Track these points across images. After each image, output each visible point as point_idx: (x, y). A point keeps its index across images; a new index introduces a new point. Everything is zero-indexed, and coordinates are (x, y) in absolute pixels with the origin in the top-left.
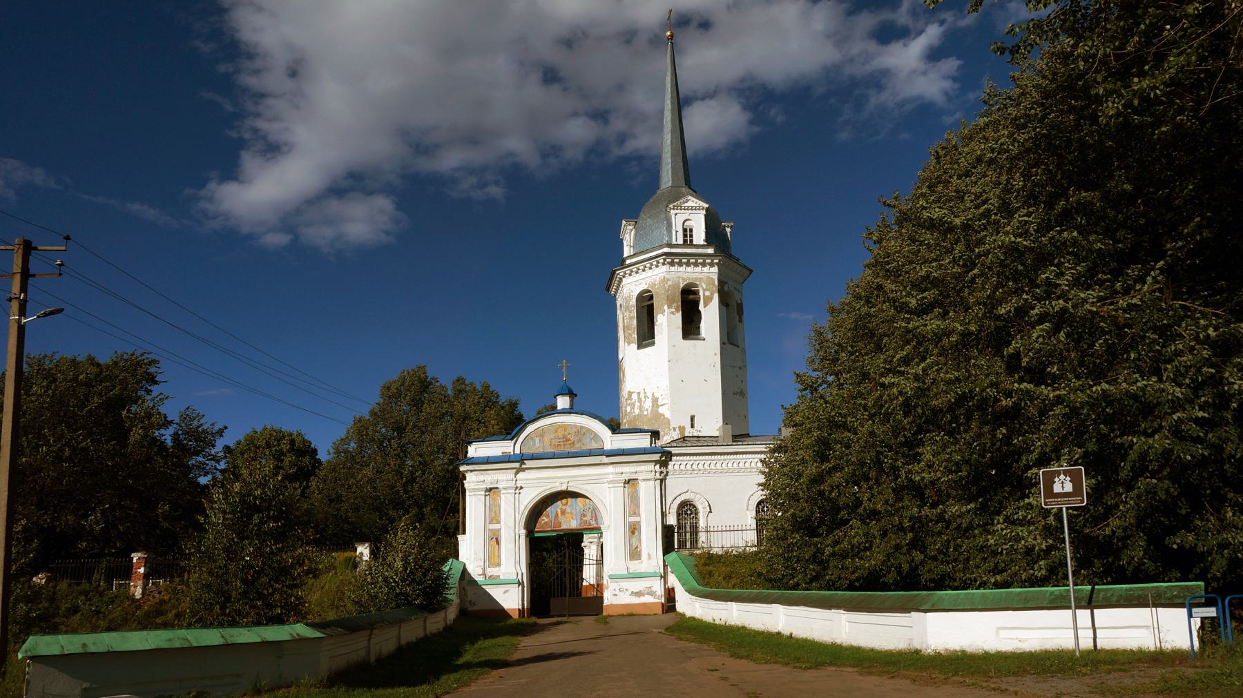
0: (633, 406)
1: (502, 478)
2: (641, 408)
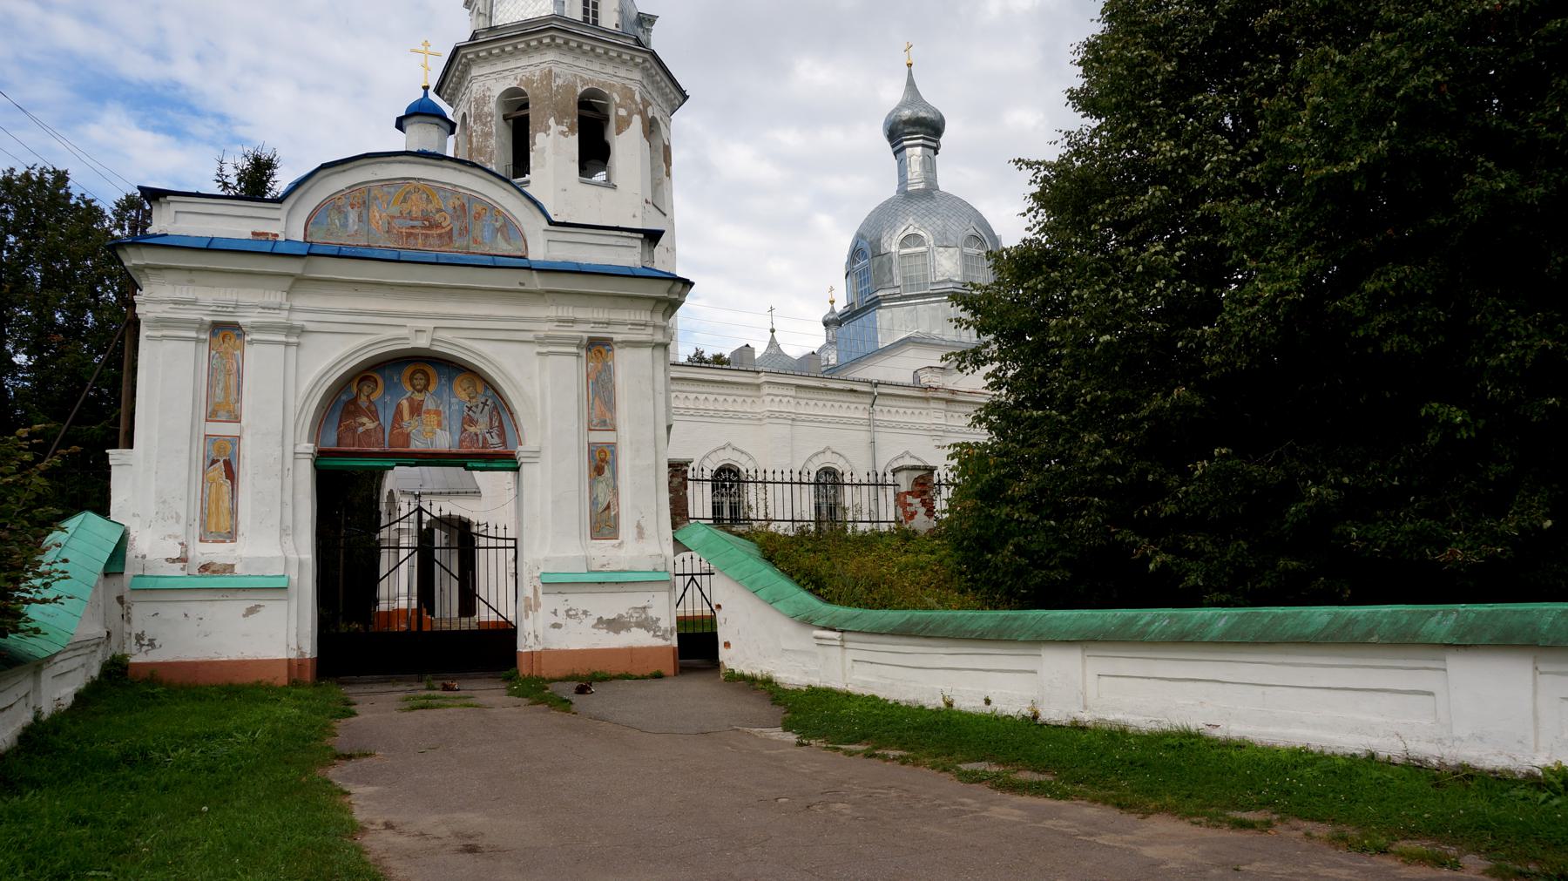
1: (251, 302)
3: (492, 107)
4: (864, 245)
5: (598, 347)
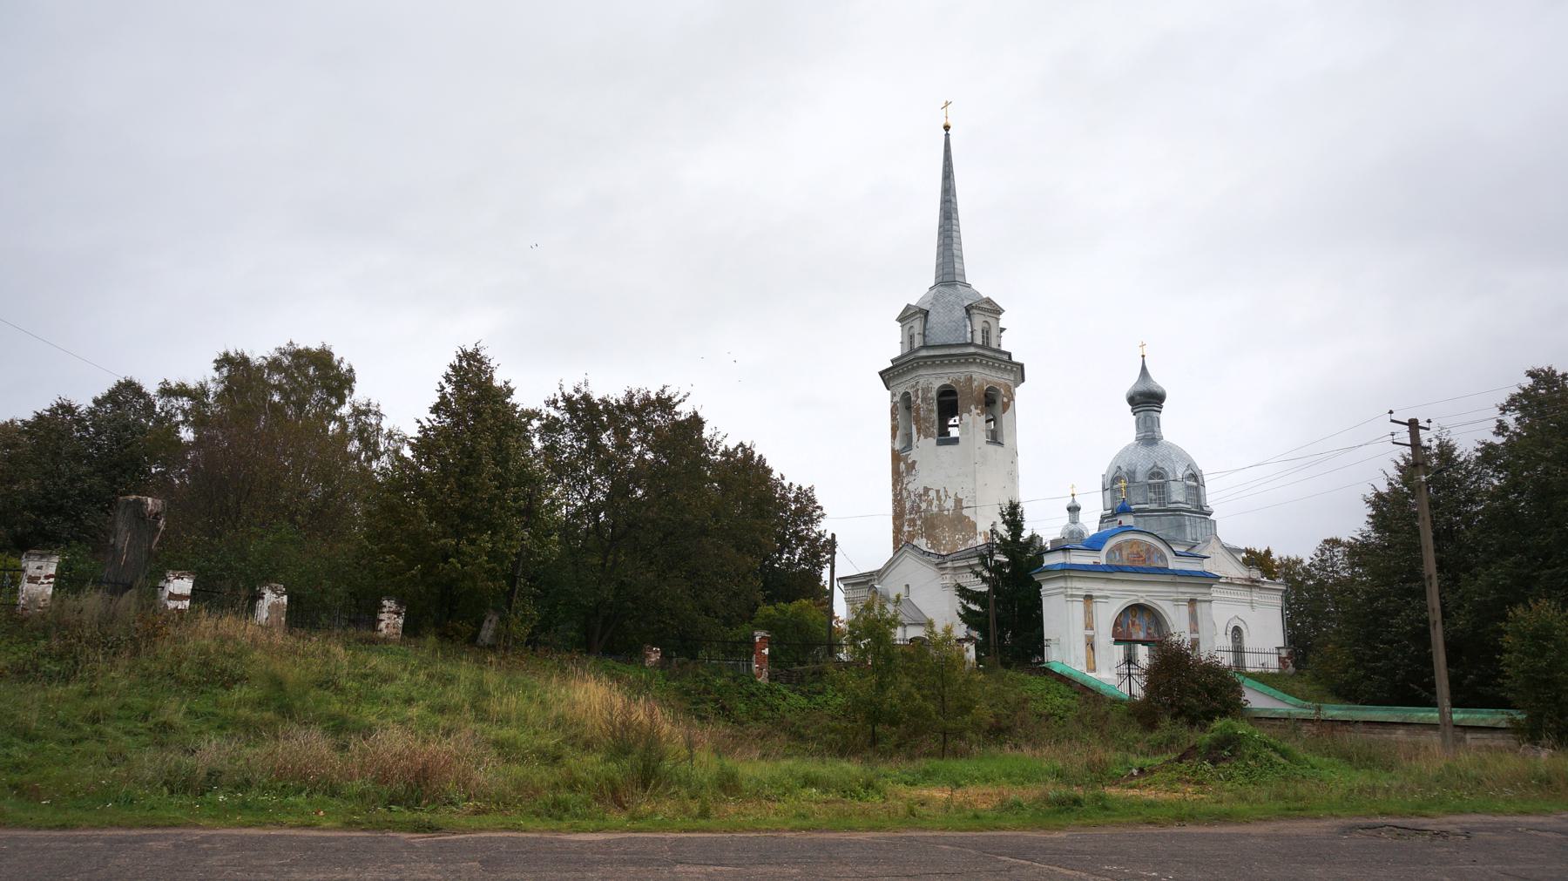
0: (930, 503)
1: (1095, 587)
2: (940, 506)
3: (934, 394)
5: (1192, 602)
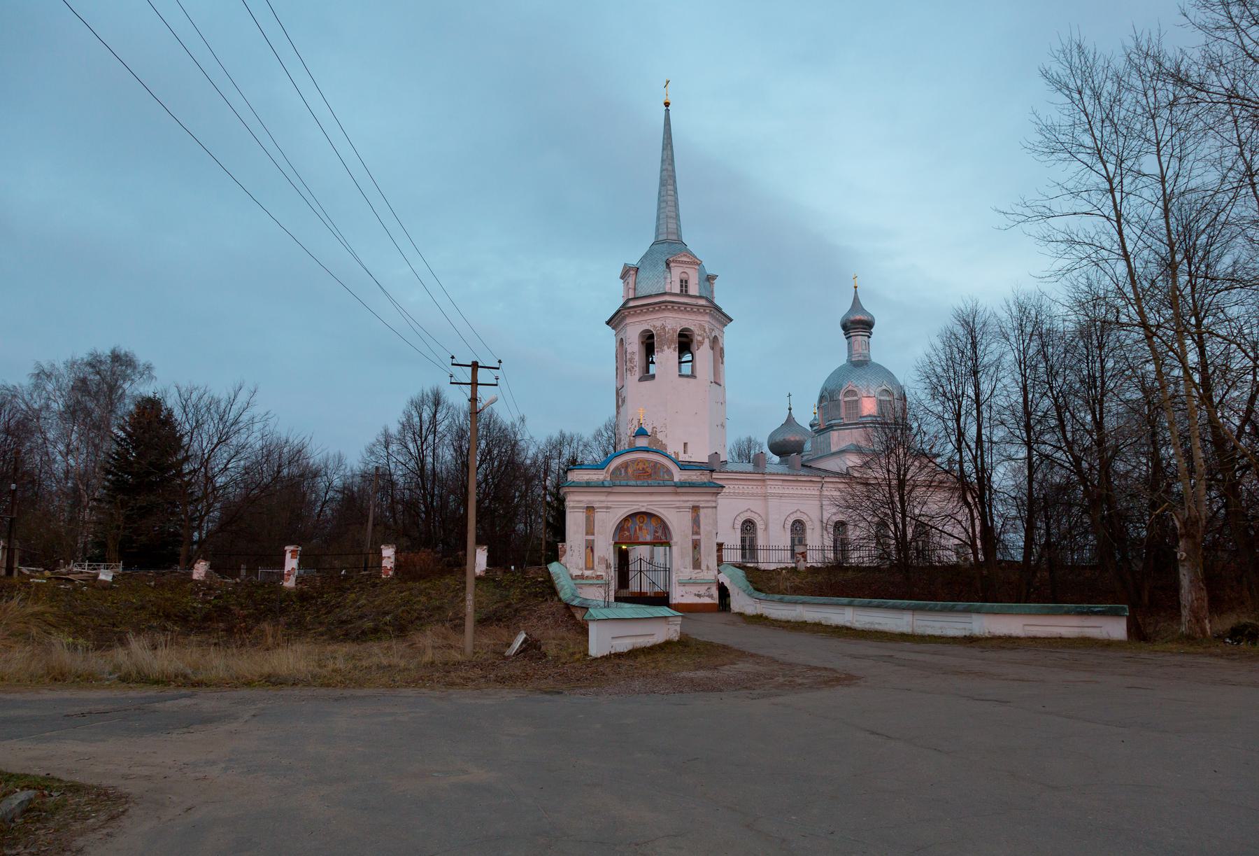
4: (826, 394)
5: (696, 509)
